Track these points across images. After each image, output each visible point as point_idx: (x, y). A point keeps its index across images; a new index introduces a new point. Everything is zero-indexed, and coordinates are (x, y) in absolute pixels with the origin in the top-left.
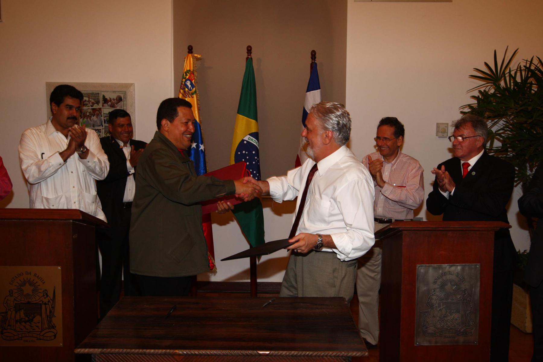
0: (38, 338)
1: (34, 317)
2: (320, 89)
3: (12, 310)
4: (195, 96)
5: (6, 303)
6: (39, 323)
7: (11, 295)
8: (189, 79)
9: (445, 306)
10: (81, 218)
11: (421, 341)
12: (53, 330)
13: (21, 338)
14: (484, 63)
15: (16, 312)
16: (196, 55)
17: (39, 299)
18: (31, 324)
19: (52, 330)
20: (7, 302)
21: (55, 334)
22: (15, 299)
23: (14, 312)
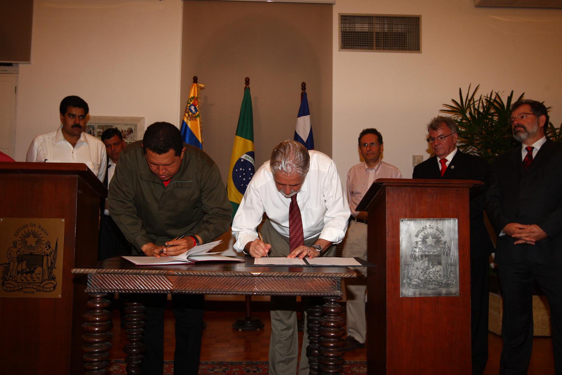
0: (37, 289)
1: (35, 269)
2: (309, 114)
3: (14, 261)
4: (198, 119)
5: (9, 255)
6: (40, 274)
7: (15, 246)
8: (193, 105)
9: (427, 258)
10: (87, 170)
11: (407, 291)
13: (21, 289)
14: (451, 100)
15: (18, 264)
16: (200, 85)
17: (42, 250)
19: (52, 281)
20: (10, 253)
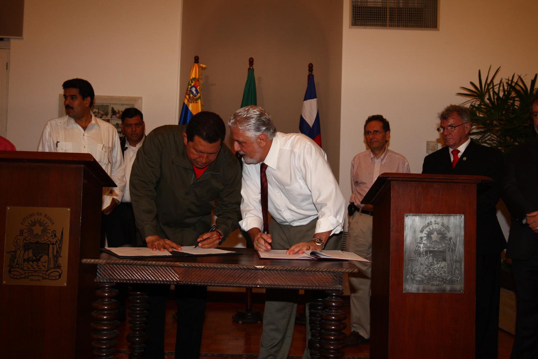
0: (43, 277)
1: (41, 257)
2: (316, 98)
3: (21, 249)
4: (199, 101)
5: (16, 243)
6: (46, 262)
7: (22, 234)
8: (194, 86)
9: (431, 254)
10: (92, 160)
11: (411, 287)
12: (59, 269)
13: (28, 277)
14: (469, 83)
15: (25, 252)
16: (202, 65)
17: (48, 239)
18: (38, 263)
19: (58, 270)
20: (17, 241)
21: (59, 273)
22: (24, 239)
23: (23, 251)
